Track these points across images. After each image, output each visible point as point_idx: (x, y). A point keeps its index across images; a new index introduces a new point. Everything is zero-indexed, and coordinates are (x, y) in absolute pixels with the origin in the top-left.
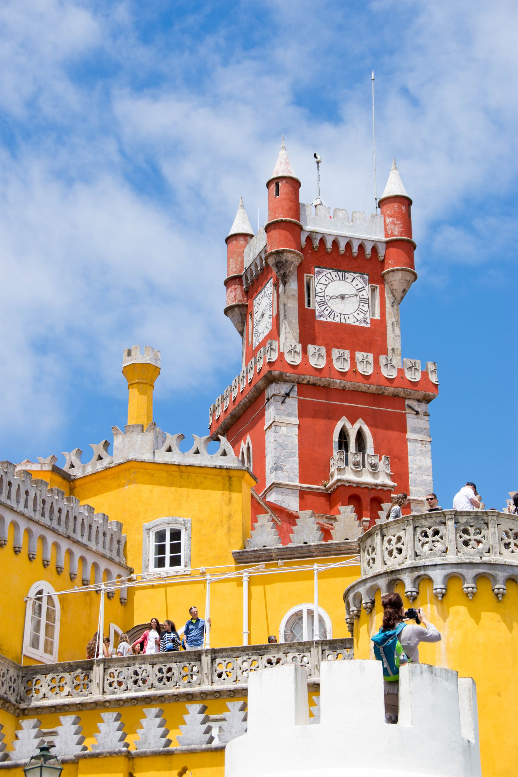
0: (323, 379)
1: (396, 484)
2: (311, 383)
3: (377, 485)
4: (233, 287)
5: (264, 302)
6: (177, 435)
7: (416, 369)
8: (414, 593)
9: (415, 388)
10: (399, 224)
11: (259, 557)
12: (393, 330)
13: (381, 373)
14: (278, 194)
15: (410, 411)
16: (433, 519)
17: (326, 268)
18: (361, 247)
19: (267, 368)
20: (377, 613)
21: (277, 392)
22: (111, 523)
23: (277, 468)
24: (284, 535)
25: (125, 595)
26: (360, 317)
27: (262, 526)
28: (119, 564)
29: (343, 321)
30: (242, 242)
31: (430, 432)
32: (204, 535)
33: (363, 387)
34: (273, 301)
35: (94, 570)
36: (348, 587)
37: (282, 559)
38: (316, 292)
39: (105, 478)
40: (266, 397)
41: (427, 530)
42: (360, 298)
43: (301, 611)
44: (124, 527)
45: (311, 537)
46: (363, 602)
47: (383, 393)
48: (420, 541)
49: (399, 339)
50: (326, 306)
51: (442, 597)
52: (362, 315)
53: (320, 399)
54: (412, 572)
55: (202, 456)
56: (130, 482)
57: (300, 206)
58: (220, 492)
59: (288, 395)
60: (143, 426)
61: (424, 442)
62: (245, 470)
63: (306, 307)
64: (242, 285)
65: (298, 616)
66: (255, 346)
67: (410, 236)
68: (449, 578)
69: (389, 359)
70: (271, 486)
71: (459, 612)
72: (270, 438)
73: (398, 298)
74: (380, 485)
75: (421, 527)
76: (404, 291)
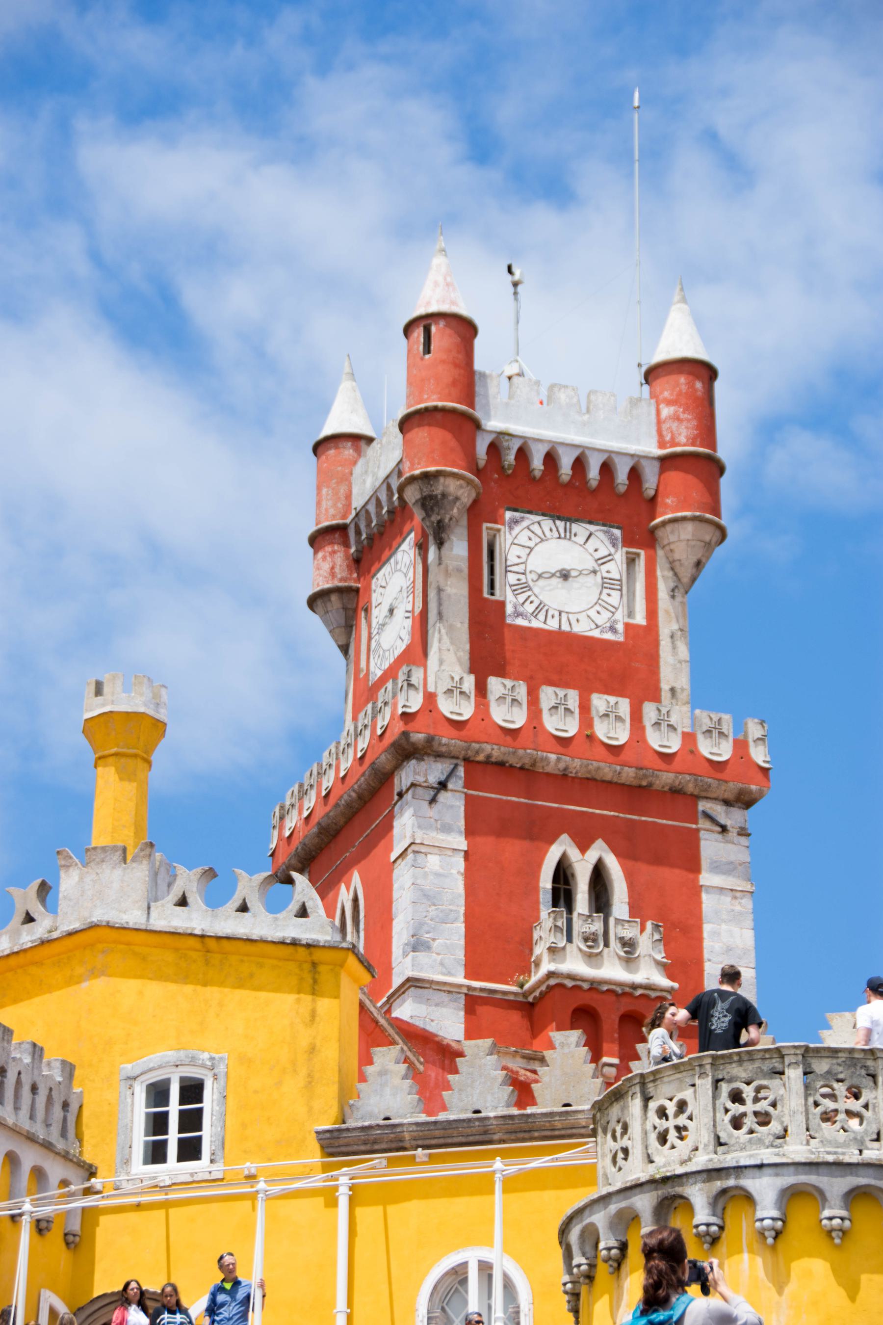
0: (521, 752)
1: (676, 985)
2: (493, 759)
3: (634, 987)
4: (329, 549)
5: (395, 583)
6: (199, 870)
7: (721, 734)
8: (714, 1228)
9: (719, 776)
10: (688, 420)
11: (375, 1142)
12: (674, 647)
13: (645, 741)
14: (427, 349)
15: (707, 824)
16: (757, 1064)
17: (530, 512)
18: (607, 468)
19: (399, 727)
20: (632, 1271)
21: (420, 779)
22: (49, 1064)
23: (417, 945)
24: (430, 1094)
25: (75, 1226)
26: (603, 618)
27: (382, 1073)
28: (66, 1156)
29: (565, 627)
30: (348, 451)
31: (750, 872)
32: (256, 1092)
33: (607, 770)
34: (414, 582)
35: (7, 1168)
36: (569, 1211)
37: (425, 1147)
38: (509, 563)
39: (39, 963)
40: (397, 790)
41: (743, 1086)
43: (465, 1265)
44: (77, 1073)
45: (489, 1098)
46: (602, 1245)
47: (650, 785)
48: (727, 1111)
49: (686, 668)
50: (529, 593)
51: (775, 1238)
52: (606, 615)
53: (516, 795)
54: (709, 1180)
55: (255, 916)
56: (94, 973)
57: (477, 378)
58: (291, 998)
59: (443, 785)
60: (124, 850)
61: (738, 894)
62: (348, 949)
63: (486, 595)
64: (346, 545)
65: (458, 1274)
66: (373, 679)
67: (712, 445)
68: (791, 1196)
70: (403, 985)
71: (813, 1272)
72: (404, 881)
73: (686, 580)
74: (640, 986)
75: (730, 1081)
76: (699, 564)
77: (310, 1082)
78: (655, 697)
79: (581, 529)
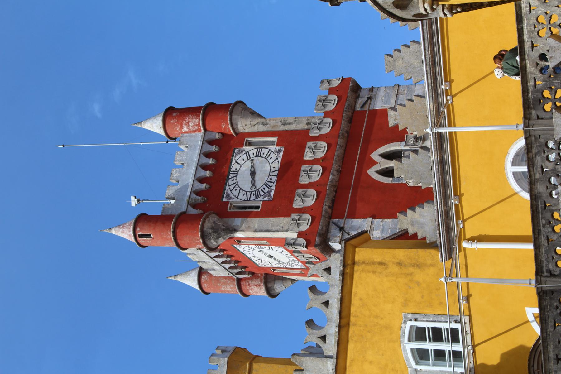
0: (328, 192)
2: (331, 205)
10: (189, 118)
15: (367, 106)
17: (225, 190)
29: (276, 173)
32: (422, 297)
33: (339, 152)
34: (255, 245)
42: (256, 156)
43: (515, 174)
47: (347, 132)
52: (272, 155)
55: (331, 298)
57: (164, 214)
61: (399, 91)
67: (201, 108)
69: (313, 126)
77: (418, 265)
78: (307, 131)
79: (234, 167)
